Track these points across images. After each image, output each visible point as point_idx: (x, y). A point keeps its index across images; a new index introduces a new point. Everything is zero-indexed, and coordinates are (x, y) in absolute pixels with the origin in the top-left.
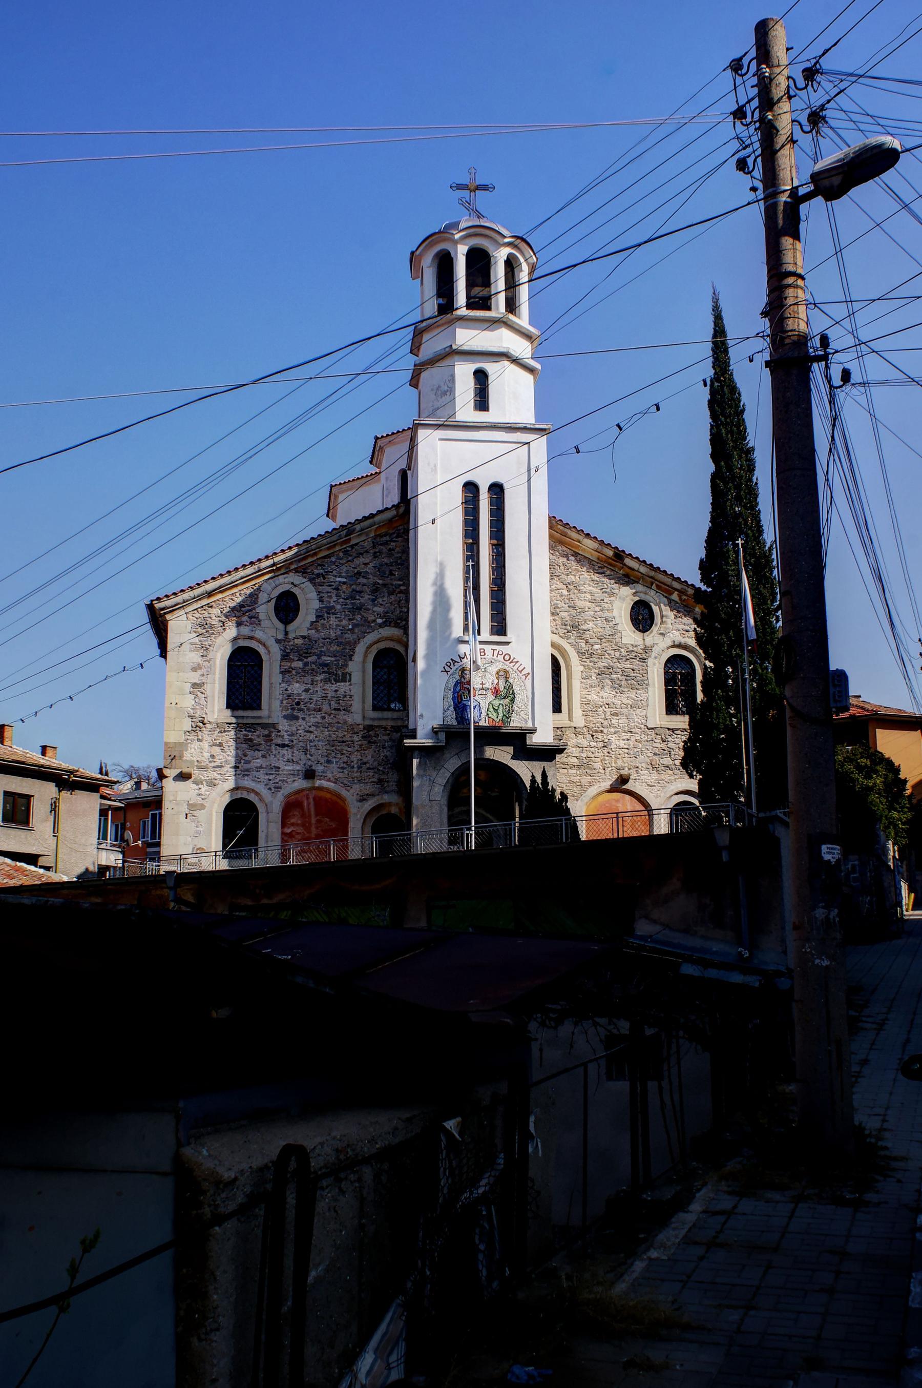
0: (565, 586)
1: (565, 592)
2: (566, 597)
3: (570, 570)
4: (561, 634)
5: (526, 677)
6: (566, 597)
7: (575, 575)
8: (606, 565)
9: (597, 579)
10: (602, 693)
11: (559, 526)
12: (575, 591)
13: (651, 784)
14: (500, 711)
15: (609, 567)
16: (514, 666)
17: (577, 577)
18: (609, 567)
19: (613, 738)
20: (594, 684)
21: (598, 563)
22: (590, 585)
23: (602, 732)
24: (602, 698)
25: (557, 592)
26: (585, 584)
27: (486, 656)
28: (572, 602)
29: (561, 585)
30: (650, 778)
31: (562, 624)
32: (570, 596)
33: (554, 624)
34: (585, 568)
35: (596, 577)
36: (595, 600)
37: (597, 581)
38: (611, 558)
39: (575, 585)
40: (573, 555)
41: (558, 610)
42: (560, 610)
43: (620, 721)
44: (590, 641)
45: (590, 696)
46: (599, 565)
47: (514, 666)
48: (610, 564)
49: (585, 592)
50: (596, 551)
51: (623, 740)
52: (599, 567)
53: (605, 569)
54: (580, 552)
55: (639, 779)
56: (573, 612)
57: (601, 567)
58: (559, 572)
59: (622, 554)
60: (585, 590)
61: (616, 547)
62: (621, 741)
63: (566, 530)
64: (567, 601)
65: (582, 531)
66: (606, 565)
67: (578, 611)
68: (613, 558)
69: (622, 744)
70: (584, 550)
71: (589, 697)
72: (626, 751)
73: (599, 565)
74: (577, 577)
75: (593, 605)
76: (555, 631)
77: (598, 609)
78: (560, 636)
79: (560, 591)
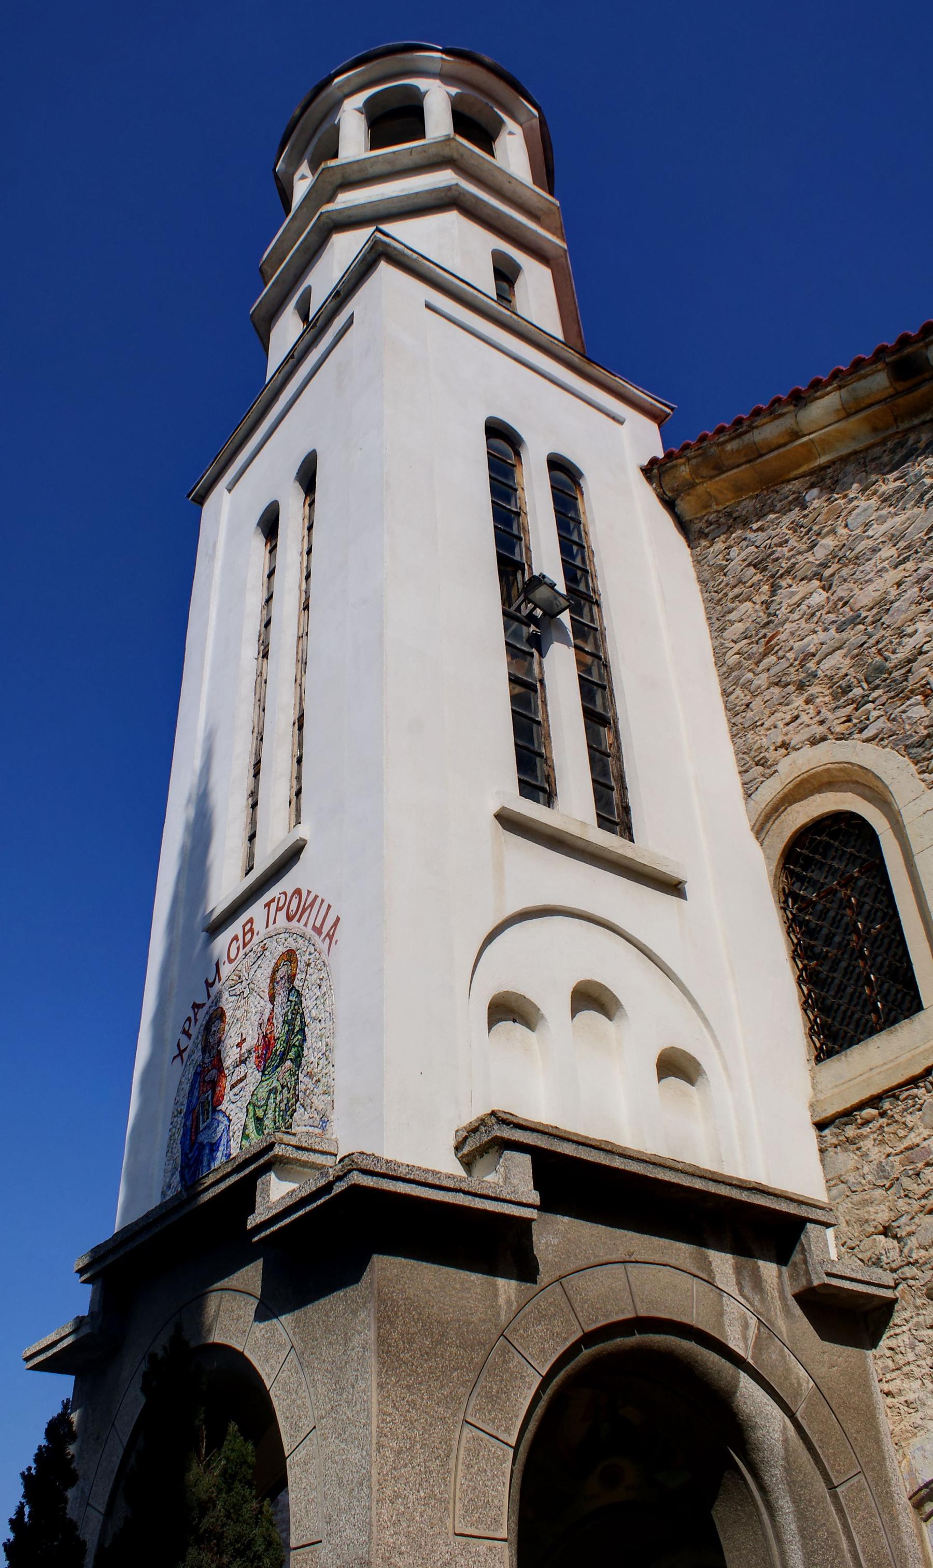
0: (816, 583)
1: (819, 597)
2: (826, 609)
3: (815, 528)
4: (839, 729)
5: (331, 938)
6: (824, 612)
7: (833, 532)
8: (904, 426)
9: (898, 483)
11: (729, 447)
12: (845, 572)
15: (916, 422)
16: (306, 925)
17: (842, 531)
18: (916, 422)
21: (884, 442)
22: (882, 520)
25: (796, 616)
26: (867, 525)
28: (847, 609)
29: (801, 589)
31: (835, 697)
32: (835, 598)
33: (812, 712)
34: (855, 486)
35: (889, 484)
36: (908, 547)
37: (896, 491)
38: (897, 394)
39: (841, 554)
40: (812, 486)
41: (811, 665)
42: (817, 658)
46: (890, 444)
47: (306, 925)
48: (914, 412)
49: (875, 550)
50: (849, 415)
52: (893, 451)
53: (912, 438)
54: (823, 460)
56: (854, 635)
57: (901, 444)
58: (789, 559)
59: (909, 350)
60: (870, 543)
61: (881, 352)
63: (747, 438)
64: (832, 617)
65: (778, 400)
66: (904, 426)
67: (869, 619)
68: (901, 386)
70: (826, 444)
73: (890, 444)
74: (842, 531)
75: (910, 565)
76: (820, 730)
78: (841, 737)
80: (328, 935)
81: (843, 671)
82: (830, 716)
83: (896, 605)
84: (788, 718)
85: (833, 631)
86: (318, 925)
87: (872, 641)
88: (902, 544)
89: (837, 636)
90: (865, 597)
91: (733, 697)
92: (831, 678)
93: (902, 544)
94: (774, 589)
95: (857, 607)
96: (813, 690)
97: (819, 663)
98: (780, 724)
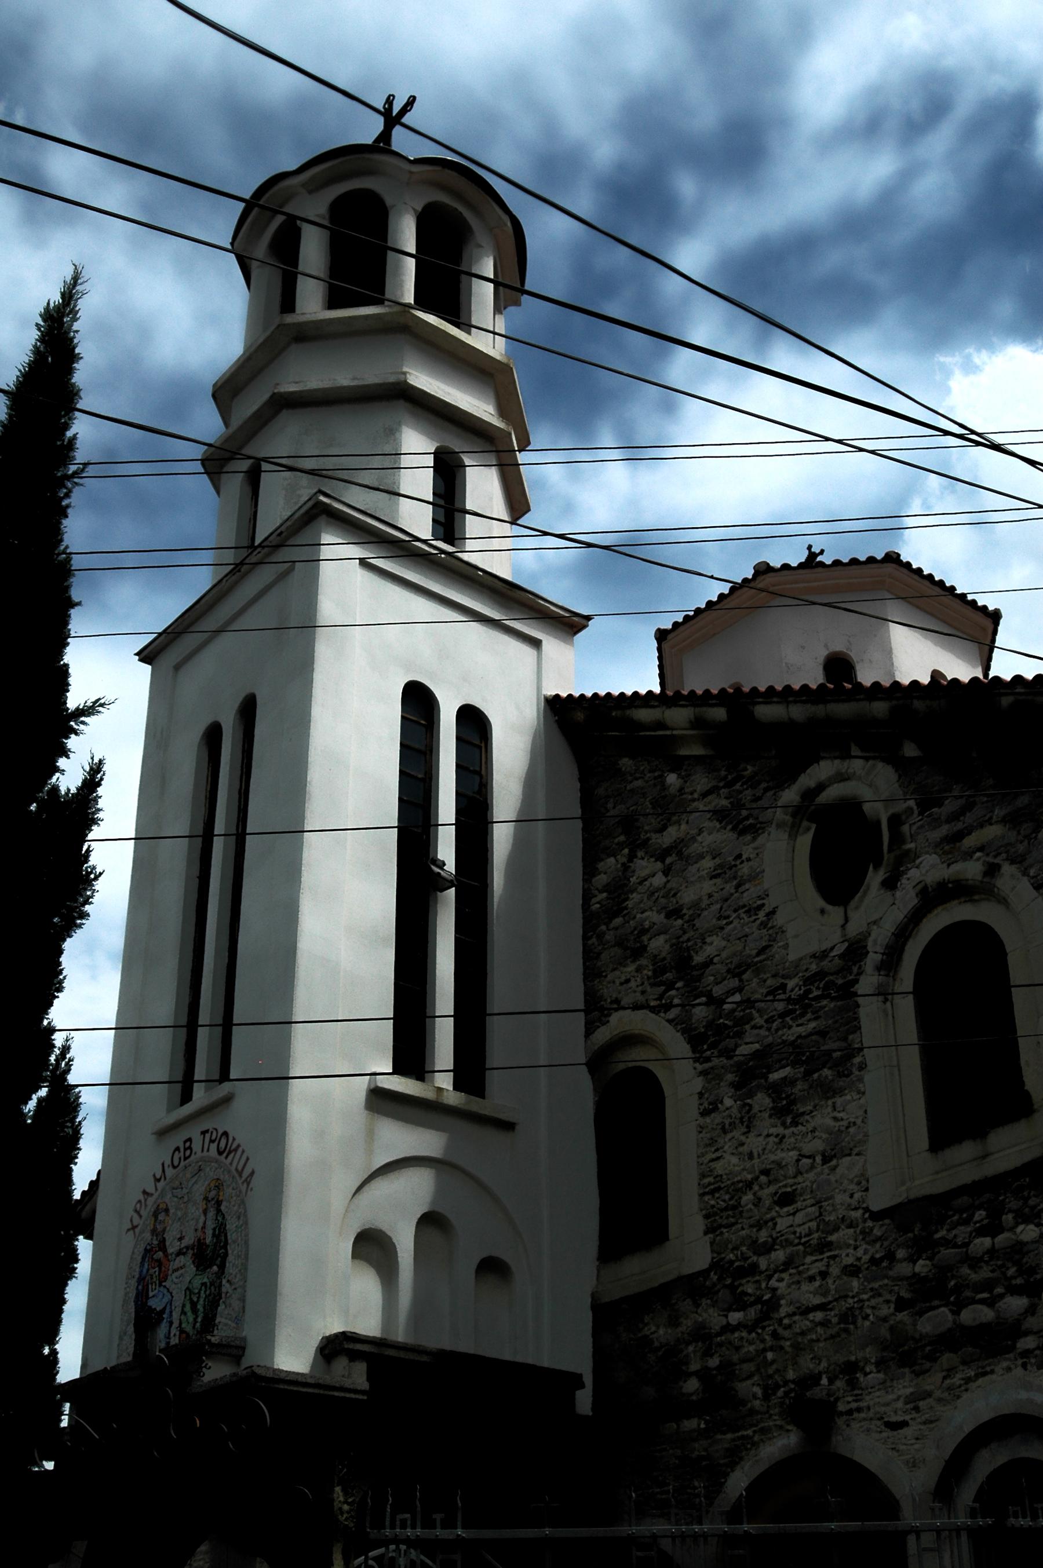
1: (659, 880)
10: (754, 1143)
13: (894, 1419)
14: (200, 1307)
16: (231, 1164)
19: (781, 1284)
20: (727, 1122)
23: (754, 1269)
24: (751, 1156)
27: (193, 1157)
30: (891, 1397)
43: (799, 1218)
44: (718, 991)
45: (721, 1163)
51: (812, 1279)
55: (859, 1410)
62: (805, 1287)
67: (687, 917)
69: (808, 1294)
71: (719, 1167)
72: (819, 1316)
76: (641, 999)
77: (730, 888)
79: (647, 883)
80: (246, 1180)
81: (663, 954)
82: (649, 989)
83: (705, 913)
84: (623, 978)
85: (662, 916)
86: (240, 1168)
87: (685, 937)
88: (718, 861)
89: (665, 921)
90: (687, 896)
91: (590, 942)
92: (655, 956)
93: (718, 861)
94: (632, 857)
95: (681, 902)
96: (643, 962)
97: (650, 939)
98: (618, 982)
